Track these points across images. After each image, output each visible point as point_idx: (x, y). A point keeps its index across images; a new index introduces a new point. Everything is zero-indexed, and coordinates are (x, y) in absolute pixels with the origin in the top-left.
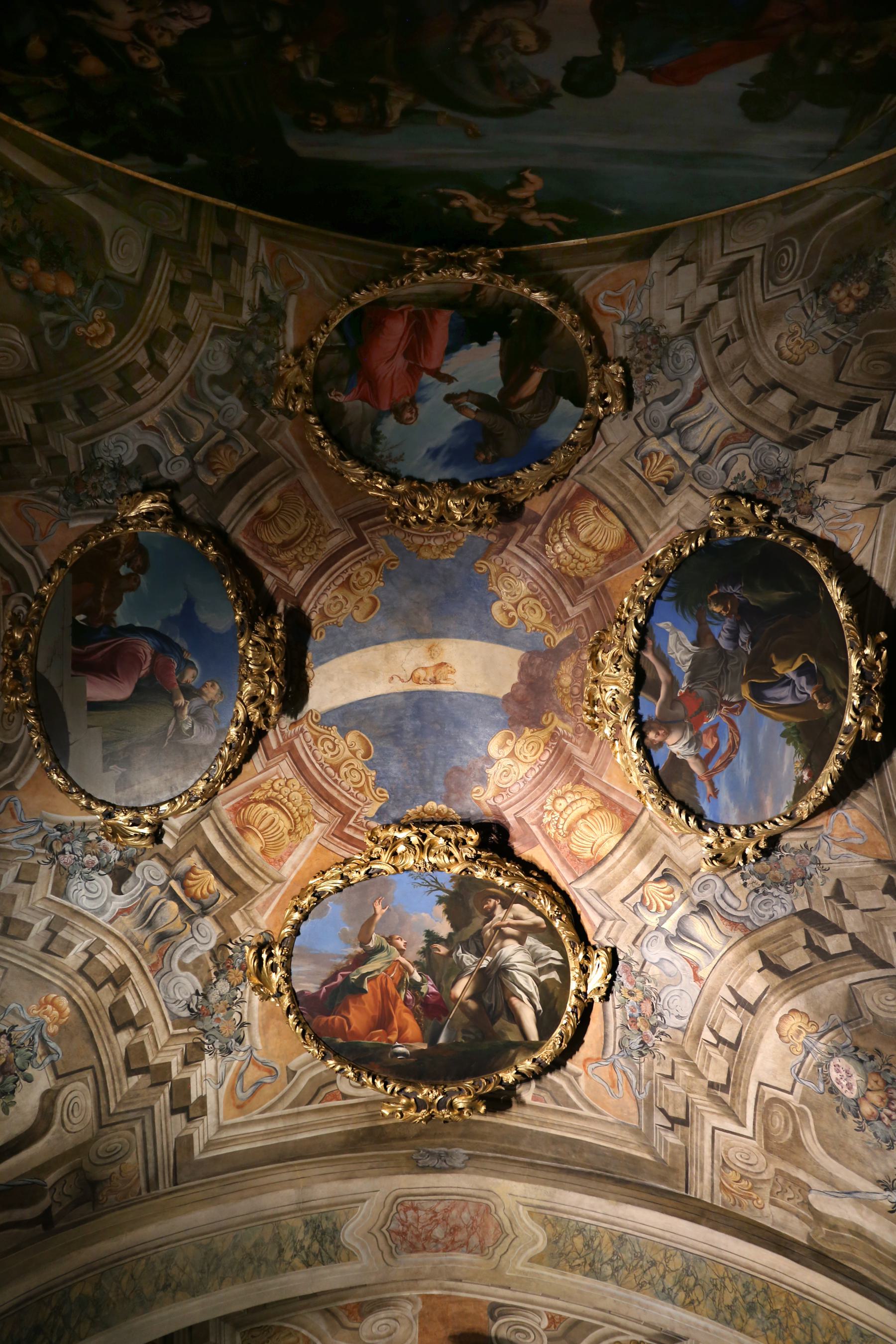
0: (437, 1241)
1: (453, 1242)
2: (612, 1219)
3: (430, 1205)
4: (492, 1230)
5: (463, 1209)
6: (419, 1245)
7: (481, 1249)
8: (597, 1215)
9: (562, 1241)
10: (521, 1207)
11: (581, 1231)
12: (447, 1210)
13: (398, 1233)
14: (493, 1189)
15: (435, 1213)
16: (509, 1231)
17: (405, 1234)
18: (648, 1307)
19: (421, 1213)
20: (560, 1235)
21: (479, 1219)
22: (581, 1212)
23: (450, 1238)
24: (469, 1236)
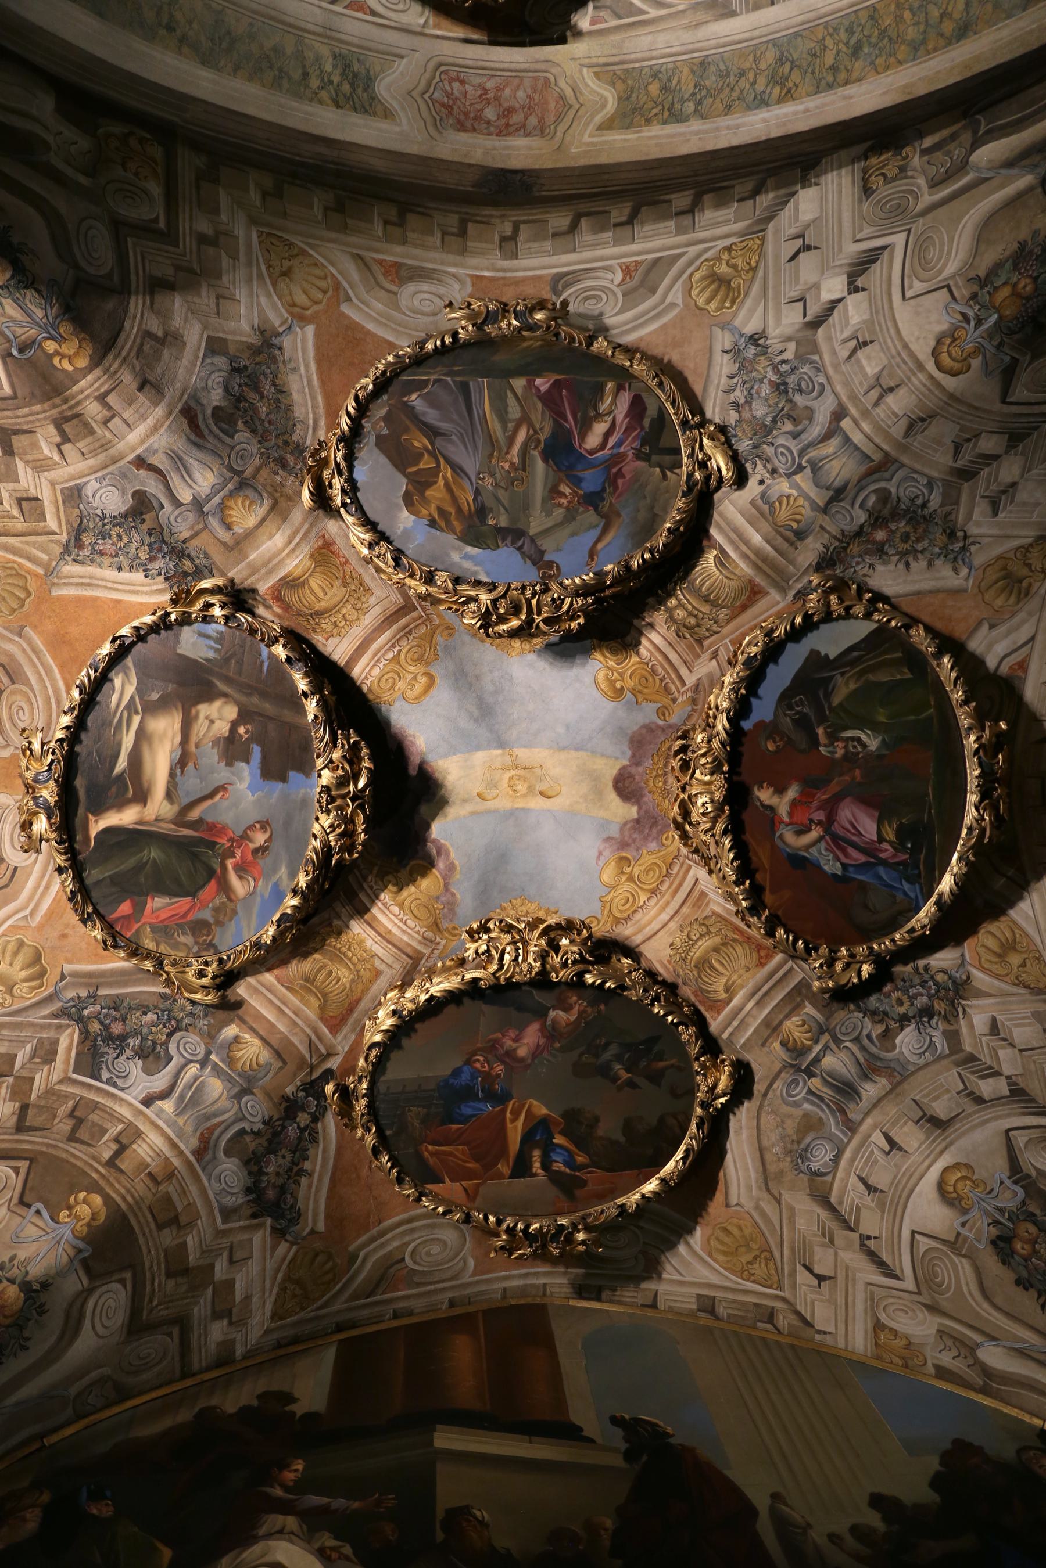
0: (488, 122)
1: (507, 125)
2: (690, 47)
3: (477, 80)
4: (552, 105)
5: (518, 88)
6: (468, 124)
7: (541, 130)
8: (674, 50)
9: (634, 95)
10: (585, 70)
11: (655, 75)
12: (498, 89)
13: (443, 105)
14: (552, 58)
15: (486, 91)
16: (571, 100)
17: (451, 107)
18: (738, 127)
19: (469, 88)
20: (632, 88)
21: (536, 97)
22: (655, 53)
23: (504, 121)
24: (526, 118)
